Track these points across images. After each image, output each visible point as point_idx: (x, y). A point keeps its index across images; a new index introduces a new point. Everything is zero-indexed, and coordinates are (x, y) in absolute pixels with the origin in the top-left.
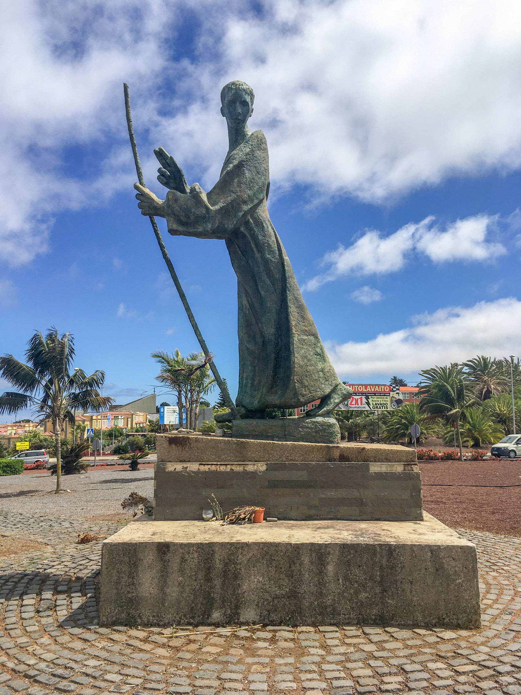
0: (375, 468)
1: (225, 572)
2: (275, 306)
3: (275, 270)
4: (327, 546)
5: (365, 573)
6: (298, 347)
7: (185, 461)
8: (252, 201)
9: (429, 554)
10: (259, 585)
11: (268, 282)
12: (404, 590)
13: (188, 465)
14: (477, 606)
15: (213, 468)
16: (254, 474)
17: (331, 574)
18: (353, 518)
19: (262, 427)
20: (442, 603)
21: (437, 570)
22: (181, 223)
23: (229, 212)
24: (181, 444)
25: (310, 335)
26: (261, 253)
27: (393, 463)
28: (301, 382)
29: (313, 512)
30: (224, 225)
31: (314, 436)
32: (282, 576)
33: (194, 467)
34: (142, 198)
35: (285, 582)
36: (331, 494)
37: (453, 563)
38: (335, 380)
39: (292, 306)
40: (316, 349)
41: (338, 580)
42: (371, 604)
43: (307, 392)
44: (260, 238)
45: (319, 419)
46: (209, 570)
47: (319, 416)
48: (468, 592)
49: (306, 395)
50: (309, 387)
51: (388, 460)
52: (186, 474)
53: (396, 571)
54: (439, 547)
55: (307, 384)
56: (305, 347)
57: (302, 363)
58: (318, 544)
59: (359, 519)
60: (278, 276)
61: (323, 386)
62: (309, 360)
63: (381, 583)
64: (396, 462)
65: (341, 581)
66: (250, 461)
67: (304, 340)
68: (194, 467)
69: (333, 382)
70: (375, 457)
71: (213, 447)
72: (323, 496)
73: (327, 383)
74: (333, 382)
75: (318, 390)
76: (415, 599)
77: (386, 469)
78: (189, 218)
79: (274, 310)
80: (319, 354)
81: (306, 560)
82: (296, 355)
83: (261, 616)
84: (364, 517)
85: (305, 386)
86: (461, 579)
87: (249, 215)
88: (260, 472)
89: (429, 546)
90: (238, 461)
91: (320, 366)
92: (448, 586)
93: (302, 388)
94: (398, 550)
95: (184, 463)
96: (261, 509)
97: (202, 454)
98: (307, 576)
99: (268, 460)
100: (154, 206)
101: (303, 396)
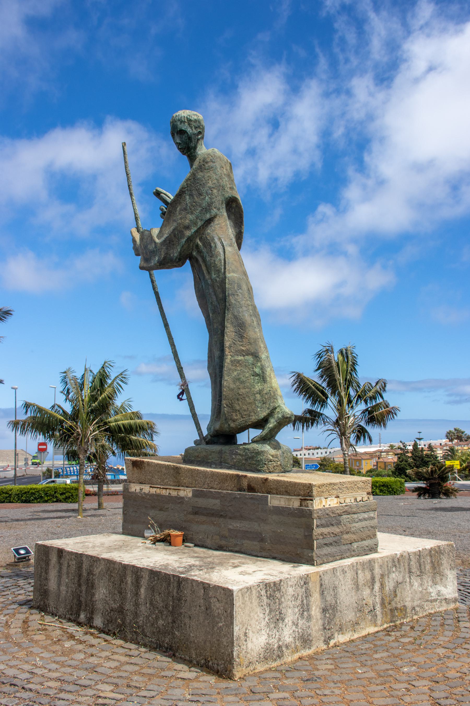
0: (275, 501)
1: (87, 580)
4: (141, 569)
5: (163, 601)
6: (230, 369)
7: (142, 483)
8: (196, 224)
9: (202, 591)
10: (104, 597)
12: (185, 624)
13: (143, 487)
14: (231, 655)
15: (158, 491)
16: (180, 500)
17: (143, 597)
18: (255, 554)
20: (208, 644)
21: (207, 609)
23: (173, 241)
25: (248, 355)
27: (291, 497)
28: (231, 406)
29: (223, 543)
30: (170, 255)
31: (244, 464)
32: (116, 592)
33: (146, 489)
35: (117, 597)
36: (236, 525)
37: (218, 605)
38: (274, 402)
39: (229, 325)
40: (255, 370)
41: (147, 604)
42: (165, 633)
43: (239, 417)
46: (80, 576)
48: (226, 638)
50: (241, 411)
51: (287, 493)
52: (140, 495)
53: (181, 603)
54: (209, 585)
55: (238, 408)
56: (239, 368)
57: (232, 386)
58: (110, 562)
59: (259, 555)
61: (259, 409)
62: (243, 382)
63: (172, 613)
64: (295, 495)
65: (148, 605)
66: (182, 486)
67: (238, 361)
68: (146, 489)
69: (271, 404)
70: (277, 489)
71: (158, 472)
72: (230, 527)
75: (252, 414)
76: (192, 635)
77: (284, 503)
81: (129, 580)
82: (226, 378)
83: (104, 625)
84: (264, 554)
85: (236, 411)
86: (222, 622)
87: (198, 238)
88: (186, 498)
89: (203, 583)
90: (175, 486)
91: (258, 387)
92: (213, 627)
93: (233, 412)
94: (183, 583)
95: (141, 485)
96: (180, 533)
98: (129, 595)
99: (195, 487)
101: (234, 421)
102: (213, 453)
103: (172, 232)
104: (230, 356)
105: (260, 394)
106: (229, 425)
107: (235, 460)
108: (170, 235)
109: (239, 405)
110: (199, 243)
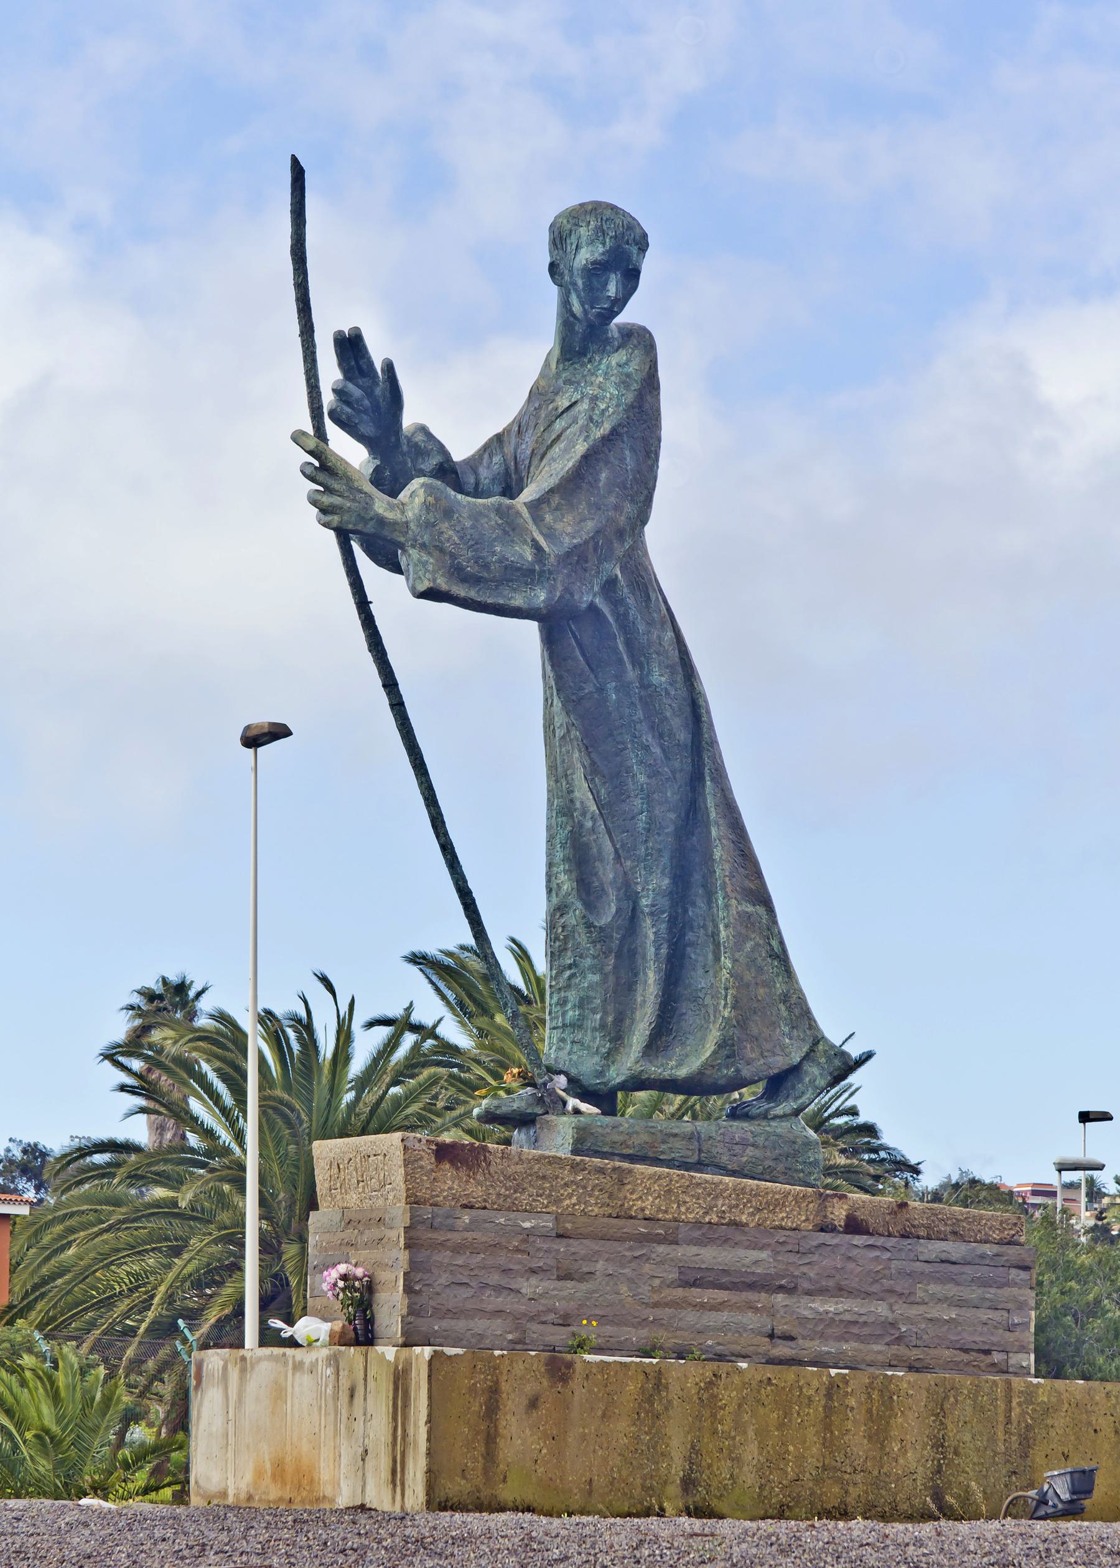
2: (672, 816)
11: (657, 750)
19: (645, 1137)
22: (458, 573)
24: (464, 1162)
26: (642, 668)
44: (642, 627)
45: (780, 1127)
49: (753, 1060)
61: (787, 1041)
74: (808, 1032)
75: (778, 1050)
78: (486, 566)
79: (670, 829)
80: (778, 957)
97: (515, 1192)
102: (672, 1139)
103: (593, 538)
105: (785, 1002)
106: (738, 1071)
107: (745, 1159)
108: (586, 542)
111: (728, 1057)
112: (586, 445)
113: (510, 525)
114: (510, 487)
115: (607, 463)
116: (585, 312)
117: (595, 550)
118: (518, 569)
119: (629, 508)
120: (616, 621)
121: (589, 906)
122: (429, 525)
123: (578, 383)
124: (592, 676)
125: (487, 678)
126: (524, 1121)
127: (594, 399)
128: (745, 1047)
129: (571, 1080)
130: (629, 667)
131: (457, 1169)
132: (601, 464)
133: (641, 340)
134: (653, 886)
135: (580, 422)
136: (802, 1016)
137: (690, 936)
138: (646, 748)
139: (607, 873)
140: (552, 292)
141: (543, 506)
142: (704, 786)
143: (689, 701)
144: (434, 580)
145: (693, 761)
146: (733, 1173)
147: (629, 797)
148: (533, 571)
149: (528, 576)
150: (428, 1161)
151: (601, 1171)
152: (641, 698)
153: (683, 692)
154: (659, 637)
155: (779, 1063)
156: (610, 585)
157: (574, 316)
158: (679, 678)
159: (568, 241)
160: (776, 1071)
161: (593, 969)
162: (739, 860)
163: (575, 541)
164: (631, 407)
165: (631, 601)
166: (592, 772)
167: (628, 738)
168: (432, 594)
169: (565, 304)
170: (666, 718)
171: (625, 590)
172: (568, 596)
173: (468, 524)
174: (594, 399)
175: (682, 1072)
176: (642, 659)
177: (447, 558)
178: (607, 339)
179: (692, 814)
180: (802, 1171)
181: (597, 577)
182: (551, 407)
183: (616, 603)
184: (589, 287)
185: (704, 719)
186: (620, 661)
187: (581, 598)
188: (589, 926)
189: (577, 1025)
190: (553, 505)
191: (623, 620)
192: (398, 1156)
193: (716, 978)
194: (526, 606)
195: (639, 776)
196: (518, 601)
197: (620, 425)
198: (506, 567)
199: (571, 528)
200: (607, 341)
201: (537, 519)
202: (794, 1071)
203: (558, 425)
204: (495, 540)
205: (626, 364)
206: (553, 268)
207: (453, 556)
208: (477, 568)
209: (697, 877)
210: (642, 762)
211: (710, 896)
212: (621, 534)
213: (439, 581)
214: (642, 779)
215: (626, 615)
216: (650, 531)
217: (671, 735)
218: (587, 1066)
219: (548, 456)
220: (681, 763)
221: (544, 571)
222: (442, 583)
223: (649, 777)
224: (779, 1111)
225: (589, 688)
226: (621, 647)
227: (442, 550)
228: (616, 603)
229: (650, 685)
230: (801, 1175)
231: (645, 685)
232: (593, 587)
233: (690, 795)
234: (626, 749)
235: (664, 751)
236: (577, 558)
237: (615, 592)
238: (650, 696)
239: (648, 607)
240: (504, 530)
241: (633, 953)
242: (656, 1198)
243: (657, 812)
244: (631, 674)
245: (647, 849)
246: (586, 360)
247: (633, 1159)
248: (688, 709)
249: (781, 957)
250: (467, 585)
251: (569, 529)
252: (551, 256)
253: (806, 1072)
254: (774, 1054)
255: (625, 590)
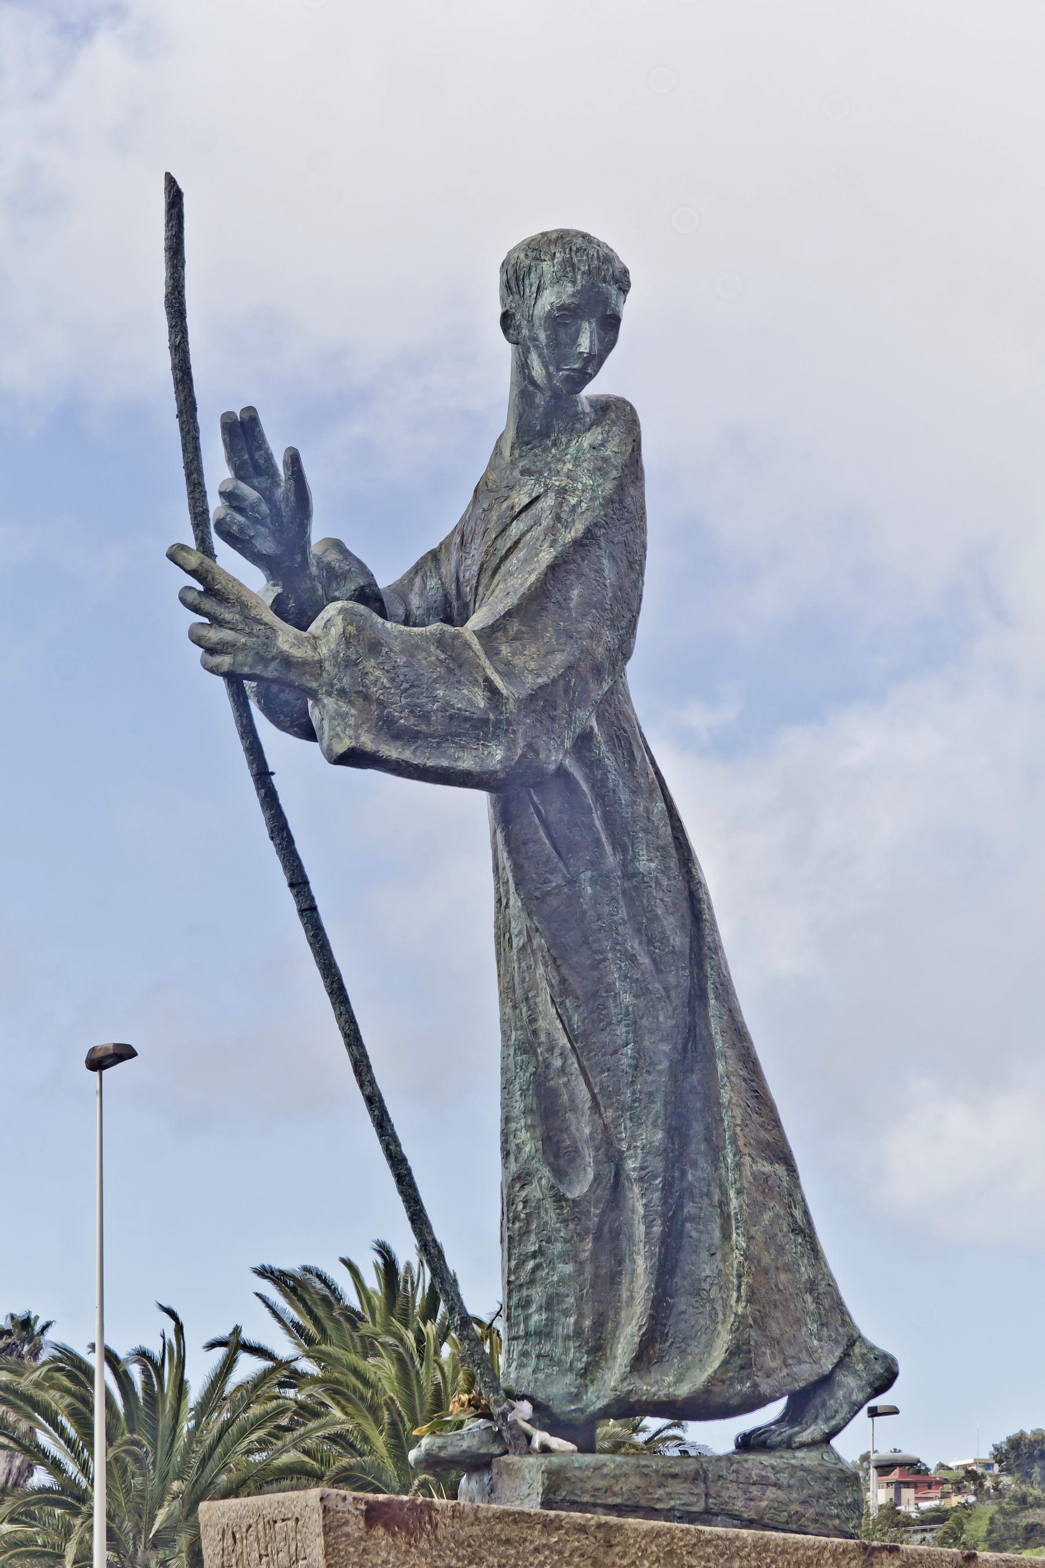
2: (666, 1047)
3: (671, 919)
11: (645, 960)
19: (636, 1481)
24: (403, 1525)
26: (625, 851)
30: (536, 752)
34: (208, 604)
44: (624, 796)
47: (802, 1446)
49: (774, 1370)
60: (679, 940)
61: (816, 1343)
73: (825, 1332)
74: (841, 1330)
75: (804, 1356)
78: (425, 717)
79: (664, 1065)
93: (765, 1345)
100: (281, 652)
102: (670, 1481)
104: (750, 1159)
105: (811, 1291)
106: (755, 1386)
107: (764, 1504)
108: (554, 681)
109: (779, 1324)
110: (596, 728)
111: (742, 1368)
112: (553, 553)
113: (455, 661)
114: (452, 610)
115: (580, 575)
116: (549, 376)
117: (566, 691)
118: (467, 719)
119: (608, 636)
120: (592, 788)
121: (560, 1173)
122: (350, 664)
123: (540, 472)
124: (561, 865)
125: (425, 865)
126: (478, 1464)
127: (562, 492)
128: (764, 1354)
129: (537, 1407)
130: (608, 849)
131: (394, 1535)
132: (573, 577)
133: (618, 414)
134: (643, 1142)
135: (544, 523)
136: (834, 1312)
137: (690, 1208)
138: (633, 958)
139: (582, 1127)
140: (504, 351)
141: (499, 634)
142: (706, 1005)
143: (686, 893)
144: (357, 737)
145: (691, 973)
146: (750, 1524)
147: (610, 1024)
148: (485, 721)
149: (481, 728)
150: (355, 1527)
151: (582, 1529)
152: (624, 892)
153: (679, 883)
154: (647, 810)
155: (806, 1373)
156: (585, 739)
157: (533, 382)
158: (673, 862)
159: (527, 282)
160: (802, 1384)
161: (564, 1257)
162: (752, 1103)
163: (540, 680)
164: (609, 501)
165: (610, 762)
166: (562, 991)
167: (607, 944)
168: (354, 758)
169: (522, 367)
170: (657, 918)
171: (603, 748)
172: (531, 755)
173: (401, 660)
174: (562, 492)
175: (684, 1390)
176: (626, 839)
177: (374, 707)
178: (577, 414)
179: (692, 1043)
180: (838, 1516)
181: (568, 728)
182: (504, 506)
183: (592, 765)
184: (555, 342)
185: (706, 917)
186: (598, 842)
187: (548, 757)
188: (559, 1199)
189: (544, 1333)
190: (511, 633)
191: (600, 787)
192: (315, 1522)
193: (720, 1265)
194: (478, 769)
195: (623, 996)
196: (467, 763)
197: (596, 525)
198: (451, 718)
199: (535, 664)
200: (576, 417)
201: (492, 653)
202: (826, 1381)
203: (515, 529)
204: (435, 681)
205: (602, 445)
206: (507, 320)
207: (381, 704)
208: (412, 720)
209: (697, 1129)
210: (626, 977)
211: (715, 1154)
212: (598, 672)
213: (363, 739)
214: (627, 999)
215: (604, 780)
216: (632, 669)
217: (664, 939)
218: (557, 1389)
219: (503, 569)
220: (678, 977)
221: (501, 721)
222: (368, 742)
223: (636, 996)
224: (806, 1436)
225: (557, 880)
226: (598, 824)
227: (366, 697)
228: (592, 765)
229: (636, 874)
230: (837, 1522)
231: (629, 874)
232: (562, 742)
233: (688, 1019)
234: (605, 959)
235: (654, 961)
236: (542, 702)
237: (590, 750)
238: (636, 888)
239: (631, 769)
240: (448, 667)
241: (616, 1234)
242: (653, 1563)
243: (646, 1043)
244: (611, 860)
245: (634, 1093)
246: (550, 443)
247: (619, 1510)
248: (685, 905)
249: (805, 1231)
250: (399, 743)
251: (532, 665)
252: (504, 304)
253: (840, 1385)
254: (800, 1362)
255: (603, 748)
